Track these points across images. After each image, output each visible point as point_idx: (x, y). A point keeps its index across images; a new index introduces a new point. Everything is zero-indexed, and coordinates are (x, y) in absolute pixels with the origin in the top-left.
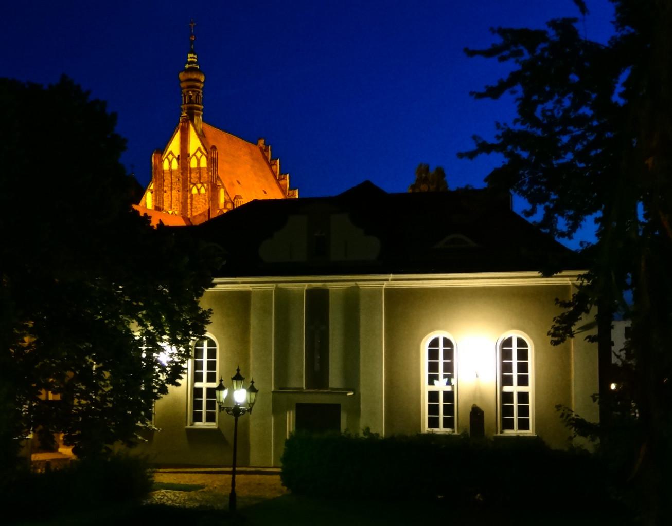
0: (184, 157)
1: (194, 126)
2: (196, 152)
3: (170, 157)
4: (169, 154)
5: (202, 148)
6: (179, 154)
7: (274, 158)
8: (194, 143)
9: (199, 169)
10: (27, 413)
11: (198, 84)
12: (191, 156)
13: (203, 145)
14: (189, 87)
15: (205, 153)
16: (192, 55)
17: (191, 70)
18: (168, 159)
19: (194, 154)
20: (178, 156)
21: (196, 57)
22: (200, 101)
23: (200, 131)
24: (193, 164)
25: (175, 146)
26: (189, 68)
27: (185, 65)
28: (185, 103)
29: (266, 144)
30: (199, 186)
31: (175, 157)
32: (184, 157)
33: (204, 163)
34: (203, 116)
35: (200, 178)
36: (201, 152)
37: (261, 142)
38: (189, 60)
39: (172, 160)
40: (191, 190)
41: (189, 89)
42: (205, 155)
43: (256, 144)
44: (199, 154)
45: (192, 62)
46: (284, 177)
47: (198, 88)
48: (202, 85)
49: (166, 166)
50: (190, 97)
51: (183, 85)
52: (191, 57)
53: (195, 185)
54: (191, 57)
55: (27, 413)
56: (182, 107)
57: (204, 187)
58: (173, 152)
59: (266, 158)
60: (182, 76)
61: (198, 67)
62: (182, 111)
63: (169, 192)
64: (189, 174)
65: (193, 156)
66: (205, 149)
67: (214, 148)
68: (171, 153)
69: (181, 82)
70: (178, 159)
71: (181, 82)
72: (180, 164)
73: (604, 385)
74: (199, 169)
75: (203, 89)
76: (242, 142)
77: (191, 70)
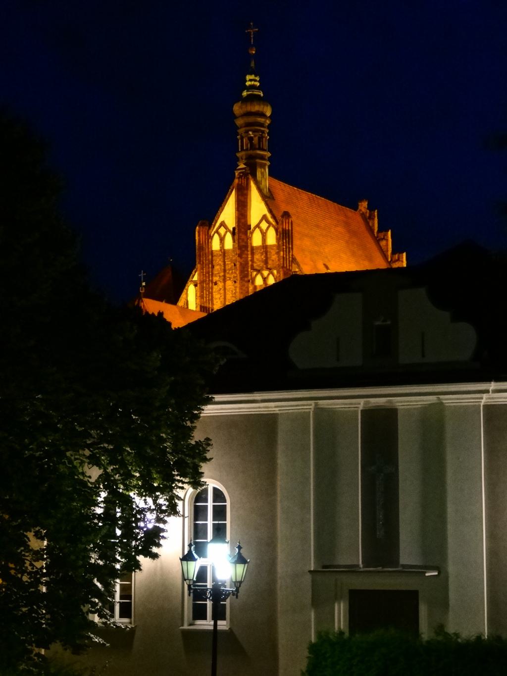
0: (242, 229)
1: (258, 184)
2: (261, 221)
3: (222, 231)
4: (220, 227)
5: (269, 216)
6: (234, 226)
7: (383, 228)
8: (257, 208)
9: (265, 247)
11: (261, 120)
12: (252, 227)
13: (270, 211)
14: (248, 125)
15: (274, 223)
16: (253, 77)
17: (252, 99)
18: (219, 234)
19: (258, 226)
20: (234, 229)
21: (258, 78)
22: (266, 145)
23: (266, 191)
24: (256, 240)
25: (228, 214)
26: (248, 95)
27: (242, 93)
28: (242, 149)
29: (371, 208)
30: (266, 273)
31: (230, 231)
32: (242, 229)
33: (272, 239)
34: (270, 167)
35: (266, 262)
36: (268, 221)
37: (364, 205)
38: (248, 83)
39: (225, 235)
40: (253, 280)
41: (248, 128)
42: (274, 226)
43: (355, 207)
44: (264, 225)
45: (252, 87)
46: (399, 258)
47: (262, 125)
48: (268, 122)
49: (216, 245)
50: (251, 139)
51: (239, 122)
52: (251, 80)
53: (259, 271)
54: (251, 80)
56: (238, 155)
57: (273, 275)
58: (227, 223)
59: (370, 230)
60: (237, 109)
61: (262, 95)
62: (238, 161)
63: (221, 285)
65: (255, 228)
66: (274, 217)
67: (286, 215)
68: (223, 224)
69: (235, 117)
70: (233, 234)
71: (235, 117)
72: (237, 242)
74: (265, 247)
75: (269, 127)
76: (332, 206)
77: (252, 99)
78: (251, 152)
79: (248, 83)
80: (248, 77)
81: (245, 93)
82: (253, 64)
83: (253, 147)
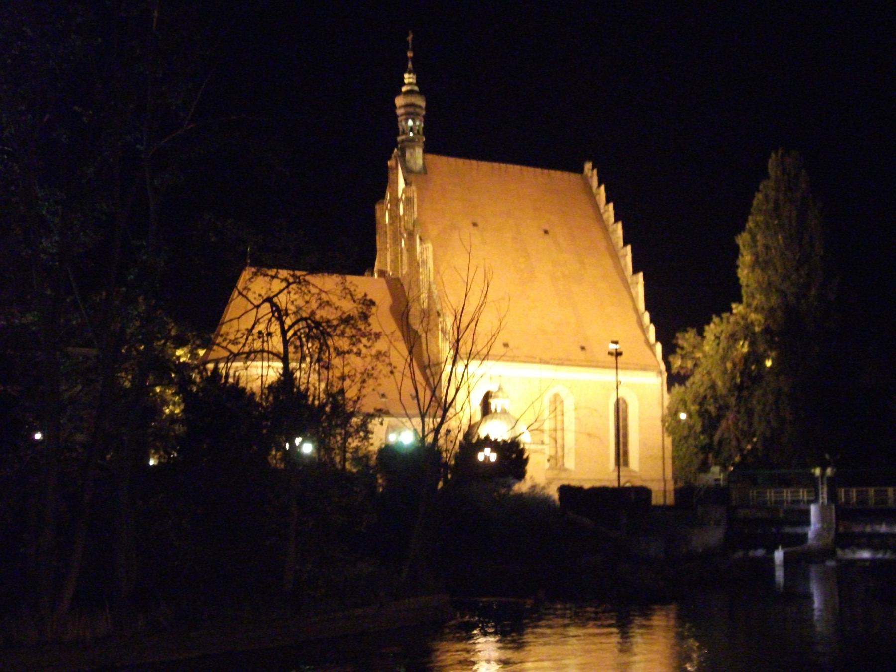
11: (418, 110)
16: (411, 75)
17: (408, 92)
41: (408, 117)
45: (410, 84)
48: (424, 113)
51: (400, 112)
54: (408, 78)
60: (399, 101)
64: (398, 224)
79: (406, 81)
80: (406, 76)
81: (404, 89)
82: (410, 65)
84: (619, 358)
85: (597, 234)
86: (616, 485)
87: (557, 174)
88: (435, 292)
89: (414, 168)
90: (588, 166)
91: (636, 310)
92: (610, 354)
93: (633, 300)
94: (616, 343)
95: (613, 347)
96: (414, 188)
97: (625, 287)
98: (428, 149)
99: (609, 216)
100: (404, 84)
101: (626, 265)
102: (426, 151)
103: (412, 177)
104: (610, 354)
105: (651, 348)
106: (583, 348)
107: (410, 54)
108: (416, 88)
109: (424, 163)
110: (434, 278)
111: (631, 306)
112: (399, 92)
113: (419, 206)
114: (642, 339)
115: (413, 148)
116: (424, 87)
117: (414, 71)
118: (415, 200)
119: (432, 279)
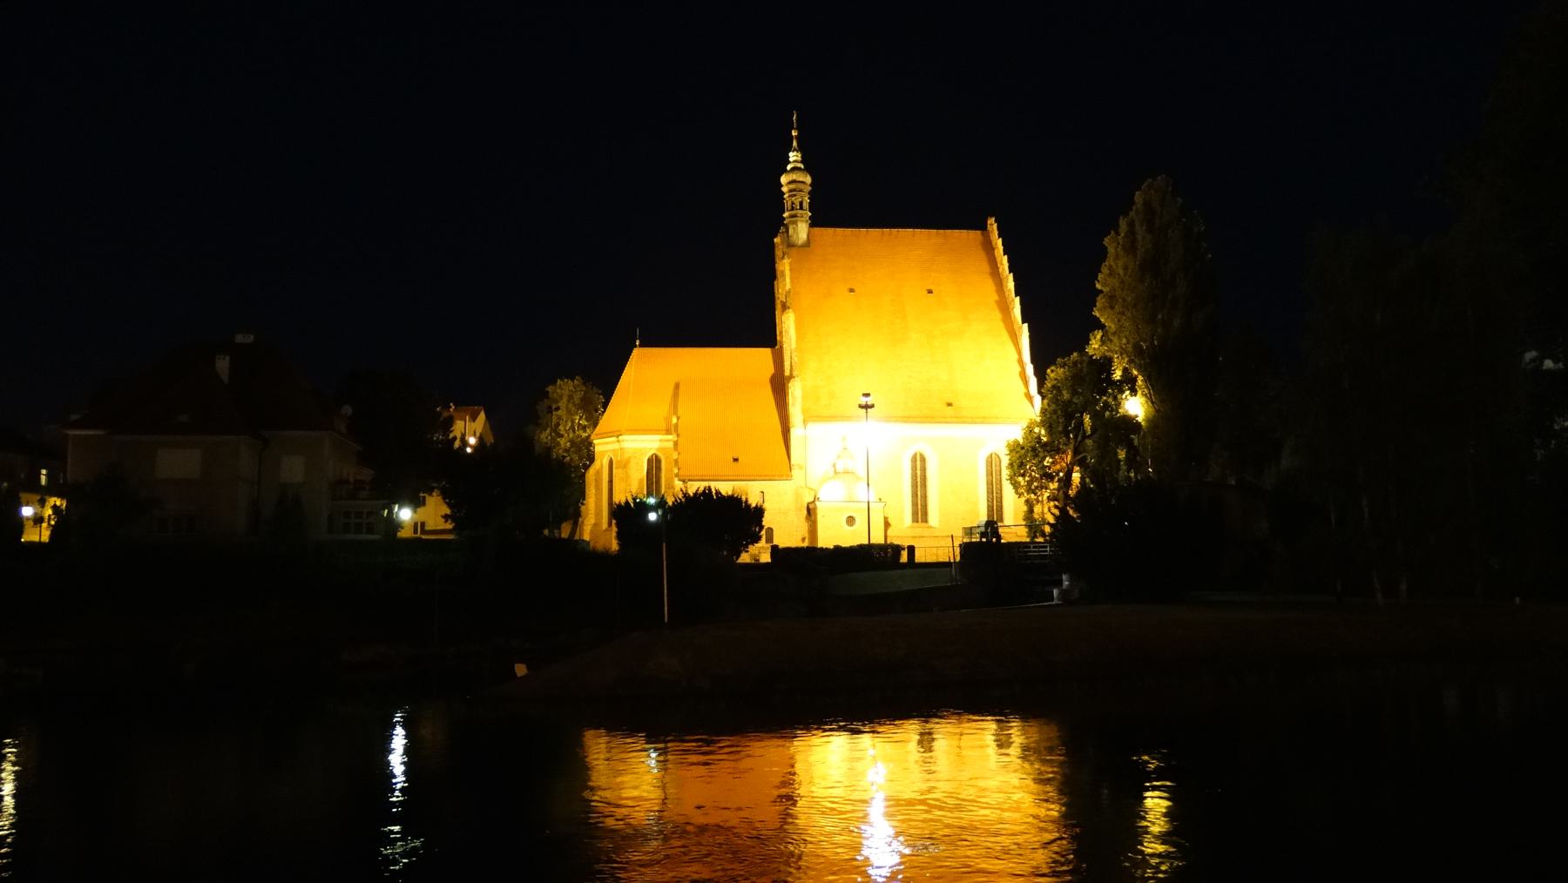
10: (61, 481)
11: (801, 186)
14: (790, 191)
16: (795, 153)
17: (794, 169)
22: (806, 205)
45: (795, 161)
48: (810, 188)
51: (785, 189)
54: (794, 156)
55: (61, 481)
56: (785, 215)
60: (784, 179)
61: (802, 167)
69: (782, 186)
71: (782, 186)
73: (589, 466)
78: (793, 212)
79: (791, 159)
80: (791, 154)
81: (789, 167)
82: (795, 144)
83: (793, 209)
84: (869, 410)
85: (990, 286)
86: (866, 542)
87: (956, 232)
88: (796, 359)
89: (796, 242)
90: (991, 221)
91: (1021, 362)
92: (861, 406)
93: (1019, 352)
94: (867, 395)
95: (863, 401)
96: (786, 261)
97: (1013, 341)
98: (815, 222)
99: (1003, 269)
100: (789, 162)
101: (1014, 316)
102: (812, 225)
103: (794, 250)
104: (861, 406)
105: (1030, 398)
106: (949, 405)
107: (794, 133)
108: (802, 167)
109: (808, 236)
110: (797, 341)
111: (1016, 356)
112: (785, 171)
113: (791, 278)
114: (1024, 390)
115: (795, 223)
116: (809, 165)
117: (801, 149)
118: (787, 273)
119: (794, 345)
